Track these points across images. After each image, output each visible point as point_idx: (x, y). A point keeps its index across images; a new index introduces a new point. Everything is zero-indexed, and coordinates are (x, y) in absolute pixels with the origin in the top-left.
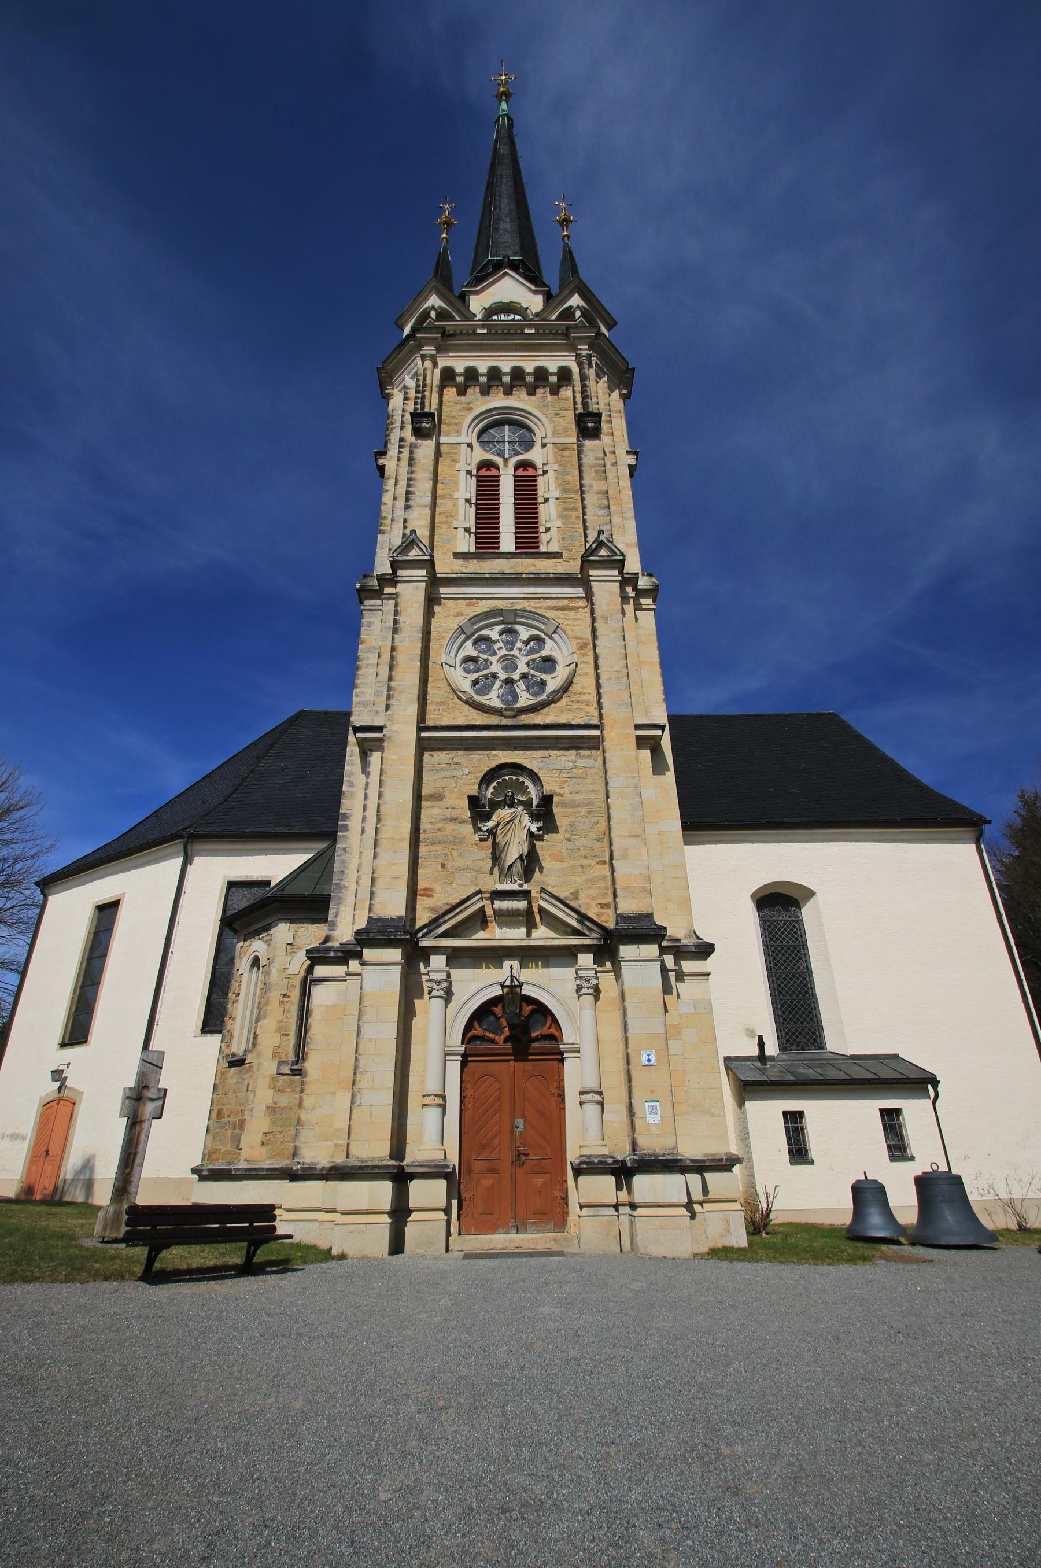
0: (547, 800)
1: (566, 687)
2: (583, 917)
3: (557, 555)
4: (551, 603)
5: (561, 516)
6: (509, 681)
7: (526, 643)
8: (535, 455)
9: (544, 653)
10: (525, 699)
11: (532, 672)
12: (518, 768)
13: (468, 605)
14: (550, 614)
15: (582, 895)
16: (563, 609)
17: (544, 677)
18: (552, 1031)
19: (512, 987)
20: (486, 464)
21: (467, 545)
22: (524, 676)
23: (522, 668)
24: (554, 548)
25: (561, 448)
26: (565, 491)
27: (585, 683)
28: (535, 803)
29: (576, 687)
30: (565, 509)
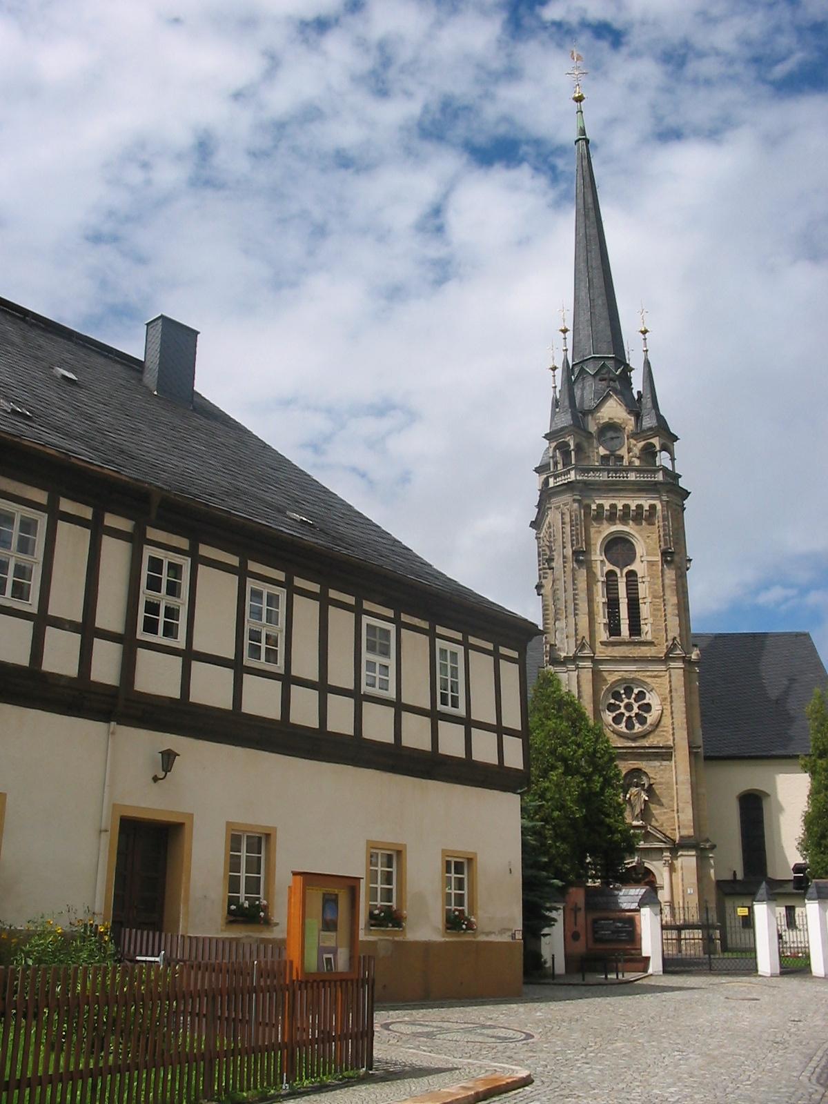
0: (651, 785)
1: (657, 724)
2: (666, 837)
3: (651, 643)
4: (648, 673)
5: (653, 615)
6: (630, 717)
7: (637, 695)
8: (637, 566)
9: (645, 701)
10: (638, 728)
11: (640, 712)
12: (639, 770)
13: (609, 674)
14: (648, 680)
15: (664, 825)
16: (655, 677)
17: (645, 715)
18: (653, 879)
19: (640, 864)
20: (611, 574)
21: (603, 635)
22: (636, 714)
23: (636, 710)
24: (649, 638)
25: (651, 564)
26: (655, 597)
27: (666, 721)
28: (646, 786)
29: (662, 723)
30: (654, 610)
